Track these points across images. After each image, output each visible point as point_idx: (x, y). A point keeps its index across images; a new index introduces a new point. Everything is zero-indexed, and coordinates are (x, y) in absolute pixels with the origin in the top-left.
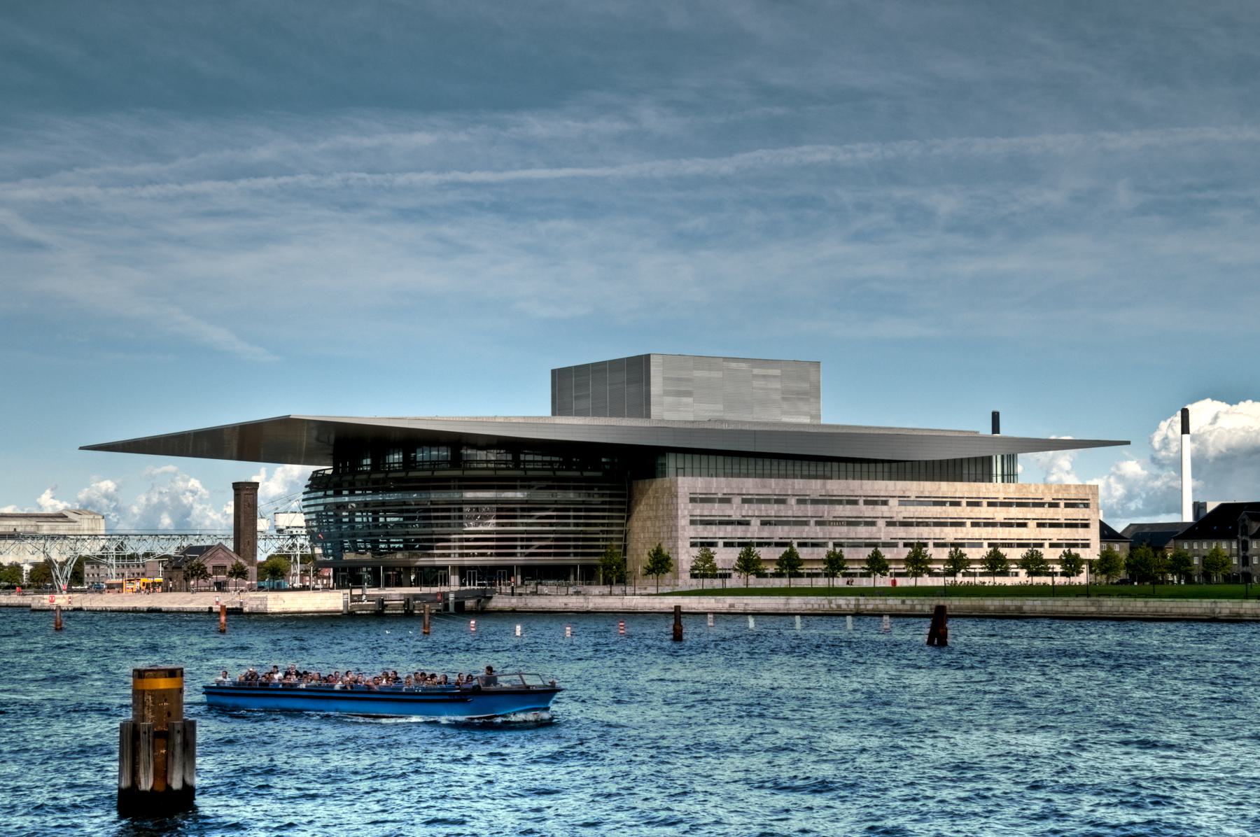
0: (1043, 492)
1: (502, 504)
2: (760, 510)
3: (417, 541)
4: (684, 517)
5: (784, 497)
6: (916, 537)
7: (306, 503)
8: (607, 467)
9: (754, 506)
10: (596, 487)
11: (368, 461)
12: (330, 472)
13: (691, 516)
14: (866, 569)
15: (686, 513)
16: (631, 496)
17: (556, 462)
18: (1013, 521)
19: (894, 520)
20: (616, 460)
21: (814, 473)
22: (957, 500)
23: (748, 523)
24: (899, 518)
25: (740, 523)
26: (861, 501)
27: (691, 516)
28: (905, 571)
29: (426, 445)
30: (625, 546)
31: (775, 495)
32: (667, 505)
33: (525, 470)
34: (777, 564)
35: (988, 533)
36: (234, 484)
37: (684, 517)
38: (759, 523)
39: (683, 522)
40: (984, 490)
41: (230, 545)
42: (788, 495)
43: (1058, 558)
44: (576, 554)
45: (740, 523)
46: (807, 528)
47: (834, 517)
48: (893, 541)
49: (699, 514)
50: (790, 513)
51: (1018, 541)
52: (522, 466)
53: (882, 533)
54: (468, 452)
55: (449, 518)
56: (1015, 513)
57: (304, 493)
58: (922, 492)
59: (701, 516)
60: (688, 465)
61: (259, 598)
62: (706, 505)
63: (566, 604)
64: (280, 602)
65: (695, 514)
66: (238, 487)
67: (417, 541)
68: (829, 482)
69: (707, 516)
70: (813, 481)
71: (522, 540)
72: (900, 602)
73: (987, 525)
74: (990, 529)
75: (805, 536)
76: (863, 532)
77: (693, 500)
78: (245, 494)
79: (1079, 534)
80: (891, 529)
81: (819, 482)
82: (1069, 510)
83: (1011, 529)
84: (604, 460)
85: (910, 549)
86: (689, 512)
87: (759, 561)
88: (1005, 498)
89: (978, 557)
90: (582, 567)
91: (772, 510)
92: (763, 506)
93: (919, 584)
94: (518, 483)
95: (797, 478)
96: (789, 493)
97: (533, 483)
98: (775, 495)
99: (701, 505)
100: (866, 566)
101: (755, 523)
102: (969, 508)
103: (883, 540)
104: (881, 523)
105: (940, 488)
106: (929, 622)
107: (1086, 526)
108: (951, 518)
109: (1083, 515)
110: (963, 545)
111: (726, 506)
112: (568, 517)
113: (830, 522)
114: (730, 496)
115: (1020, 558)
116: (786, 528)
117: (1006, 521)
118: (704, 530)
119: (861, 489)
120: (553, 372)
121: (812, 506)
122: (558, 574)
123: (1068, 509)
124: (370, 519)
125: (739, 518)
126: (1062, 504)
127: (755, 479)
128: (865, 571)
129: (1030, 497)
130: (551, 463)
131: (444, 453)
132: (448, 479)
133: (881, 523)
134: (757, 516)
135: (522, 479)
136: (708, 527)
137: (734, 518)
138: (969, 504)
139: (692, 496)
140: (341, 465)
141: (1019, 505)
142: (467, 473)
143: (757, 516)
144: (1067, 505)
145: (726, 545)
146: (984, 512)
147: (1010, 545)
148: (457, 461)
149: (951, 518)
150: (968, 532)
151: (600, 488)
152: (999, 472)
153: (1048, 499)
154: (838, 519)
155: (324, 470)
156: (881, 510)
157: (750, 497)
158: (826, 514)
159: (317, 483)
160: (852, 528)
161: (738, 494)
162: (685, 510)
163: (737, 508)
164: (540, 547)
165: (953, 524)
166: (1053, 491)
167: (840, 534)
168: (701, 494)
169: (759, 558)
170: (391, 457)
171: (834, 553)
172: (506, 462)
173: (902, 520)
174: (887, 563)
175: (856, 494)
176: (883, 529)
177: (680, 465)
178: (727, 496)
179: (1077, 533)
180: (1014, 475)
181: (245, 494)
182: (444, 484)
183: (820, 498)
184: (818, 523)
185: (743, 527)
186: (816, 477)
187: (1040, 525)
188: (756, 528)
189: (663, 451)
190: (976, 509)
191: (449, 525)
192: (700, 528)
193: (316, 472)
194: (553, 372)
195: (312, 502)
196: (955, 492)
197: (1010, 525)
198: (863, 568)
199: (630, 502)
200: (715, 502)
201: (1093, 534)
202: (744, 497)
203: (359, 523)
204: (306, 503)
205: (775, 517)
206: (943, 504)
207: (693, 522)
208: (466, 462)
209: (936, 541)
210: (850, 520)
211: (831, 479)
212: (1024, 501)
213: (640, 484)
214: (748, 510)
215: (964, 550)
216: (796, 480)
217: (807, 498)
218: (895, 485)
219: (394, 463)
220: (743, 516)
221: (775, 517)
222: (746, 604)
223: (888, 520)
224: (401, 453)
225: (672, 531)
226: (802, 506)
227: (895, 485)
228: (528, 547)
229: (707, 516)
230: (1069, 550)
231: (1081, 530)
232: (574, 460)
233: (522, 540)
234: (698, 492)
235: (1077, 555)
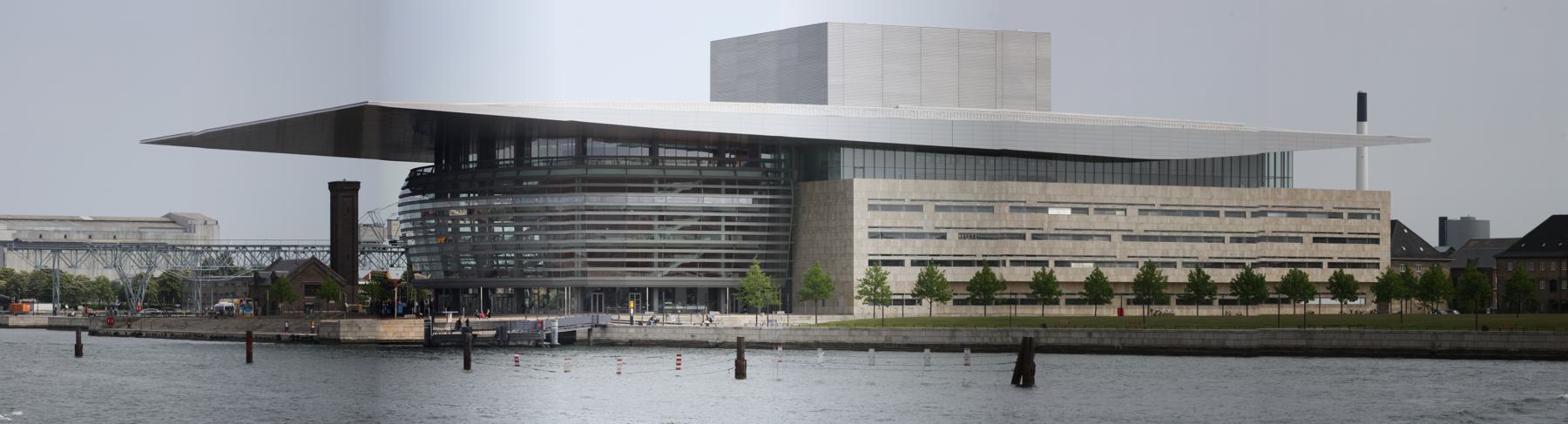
0: (1321, 200)
1: (634, 210)
2: (959, 220)
3: (540, 256)
4: (862, 228)
5: (990, 204)
6: (1161, 255)
7: (402, 209)
8: (768, 165)
9: (951, 215)
10: (756, 190)
11: (473, 157)
12: (429, 170)
14: (1085, 294)
15: (864, 223)
16: (797, 201)
17: (705, 159)
18: (1284, 235)
19: (1134, 234)
20: (783, 157)
21: (1025, 173)
22: (1214, 209)
23: (944, 237)
24: (1139, 231)
25: (932, 235)
26: (1091, 211)
28: (965, 297)
29: (542, 138)
30: (791, 264)
31: (978, 201)
32: (841, 214)
33: (664, 168)
34: (968, 289)
35: (1251, 251)
36: (329, 183)
37: (862, 228)
38: (957, 236)
39: (860, 235)
40: (1248, 198)
41: (326, 259)
42: (995, 202)
43: (1327, 281)
44: (728, 275)
45: (932, 235)
46: (1021, 242)
47: (1056, 229)
48: (1131, 260)
49: (879, 225)
50: (997, 225)
51: (1289, 260)
52: (660, 164)
53: (1121, 249)
54: (594, 147)
55: (572, 227)
56: (1287, 224)
57: (401, 197)
58: (1169, 199)
59: (882, 227)
60: (869, 163)
61: (331, 323)
62: (890, 214)
63: (692, 336)
64: (355, 329)
66: (335, 187)
67: (540, 256)
68: (1050, 185)
69: (891, 227)
70: (1030, 184)
71: (660, 255)
72: (1085, 335)
73: (1251, 240)
74: (1254, 246)
75: (1018, 253)
76: (1093, 247)
77: (872, 207)
78: (344, 196)
79: (1367, 251)
80: (1129, 244)
81: (1038, 185)
82: (1355, 222)
83: (1280, 244)
84: (764, 156)
85: (918, 270)
87: (945, 284)
88: (1274, 207)
89: (1125, 279)
90: (732, 290)
91: (975, 220)
92: (962, 215)
93: (1098, 314)
94: (656, 185)
95: (1013, 180)
96: (996, 199)
97: (674, 185)
98: (978, 201)
99: (883, 213)
100: (1084, 291)
101: (952, 236)
102: (1228, 219)
103: (1118, 259)
104: (1116, 237)
105: (1191, 194)
106: (1014, 358)
107: (1376, 241)
108: (1205, 232)
109: (1372, 228)
110: (995, 264)
111: (916, 214)
112: (718, 228)
113: (1051, 235)
114: (920, 203)
115: (1280, 280)
116: (992, 242)
117: (1274, 234)
119: (1092, 195)
120: (715, 46)
121: (1029, 214)
122: (714, 299)
123: (1353, 220)
124: (477, 229)
125: (932, 230)
126: (1345, 216)
127: (955, 182)
128: (1084, 297)
129: (1306, 204)
130: (699, 160)
131: (566, 147)
132: (571, 180)
133: (1116, 237)
134: (954, 228)
135: (661, 181)
136: (892, 240)
137: (925, 230)
138: (1228, 214)
139: (871, 202)
140: (444, 162)
141: (1291, 214)
142: (593, 172)
143: (954, 228)
144: (1351, 216)
145: (914, 263)
146: (1249, 225)
147: (1219, 265)
148: (581, 156)
149: (1205, 232)
150: (1062, 248)
151: (761, 192)
152: (1272, 174)
153: (1328, 208)
154: (1061, 232)
155: (423, 168)
156: (1118, 220)
157: (945, 204)
158: (1046, 226)
159: (415, 183)
160: (1078, 242)
161: (931, 201)
162: (862, 219)
163: (928, 217)
164: (684, 265)
165: (1209, 240)
166: (1334, 199)
167: (1064, 250)
168: (882, 200)
169: (943, 279)
170: (501, 151)
171: (1043, 274)
172: (642, 158)
173: (1143, 234)
174: (1112, 286)
175: (1084, 201)
176: (1118, 246)
177: (859, 163)
179: (1364, 250)
180: (1288, 178)
181: (344, 196)
182: (565, 186)
183: (1039, 205)
184: (1035, 237)
185: (938, 242)
186: (1037, 179)
187: (1316, 240)
188: (954, 242)
189: (836, 146)
190: (1238, 220)
191: (572, 237)
193: (414, 171)
194: (715, 46)
195: (408, 208)
196: (1211, 199)
197: (1280, 239)
198: (1081, 293)
199: (796, 209)
200: (901, 210)
201: (1383, 252)
202: (938, 204)
203: (466, 233)
204: (402, 209)
205: (978, 228)
206: (1196, 214)
207: (873, 236)
208: (593, 157)
209: (1186, 260)
211: (1056, 181)
212: (1297, 210)
213: (813, 189)
214: (943, 220)
215: (994, 269)
216: (1010, 183)
217: (1022, 205)
218: (1135, 189)
219: (504, 160)
220: (939, 228)
221: (978, 228)
222: (905, 337)
223: (1125, 233)
224: (513, 147)
225: (845, 246)
226: (1016, 215)
227: (1135, 189)
228: (666, 265)
229: (891, 227)
230: (1341, 271)
231: (1368, 247)
232: (727, 156)
233: (660, 255)
234: (879, 198)
235: (1351, 277)
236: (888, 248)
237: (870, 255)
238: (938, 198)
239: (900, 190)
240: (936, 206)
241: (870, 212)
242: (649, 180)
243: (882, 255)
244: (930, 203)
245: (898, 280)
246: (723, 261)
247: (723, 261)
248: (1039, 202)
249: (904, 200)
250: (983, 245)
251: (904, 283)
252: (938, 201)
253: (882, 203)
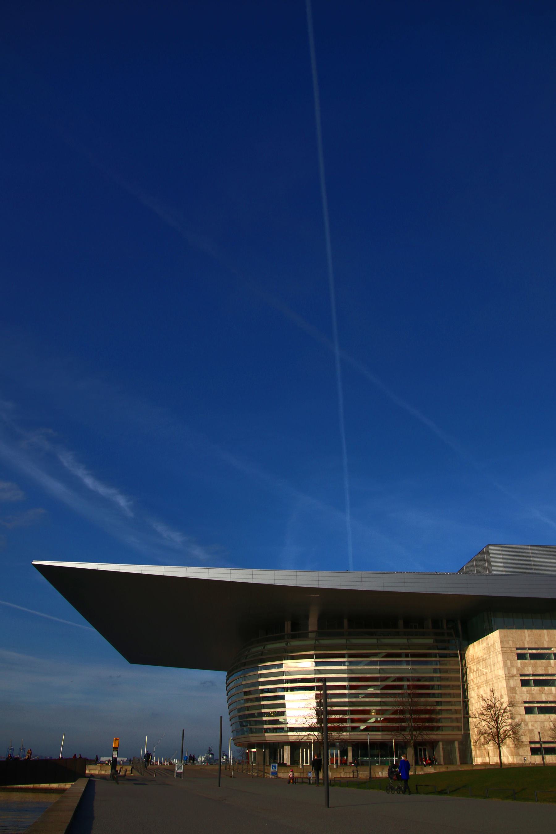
4: (513, 676)
13: (521, 675)
15: (514, 671)
27: (521, 675)
37: (513, 676)
59: (534, 675)
62: (539, 662)
65: (528, 673)
77: (521, 657)
86: (518, 669)
118: (541, 692)
136: (546, 688)
168: (530, 649)
192: (535, 689)
207: (525, 683)
234: (526, 646)
236: (543, 695)
237: (525, 702)
239: (547, 639)
241: (519, 661)
243: (538, 702)
249: (549, 649)
253: (530, 651)
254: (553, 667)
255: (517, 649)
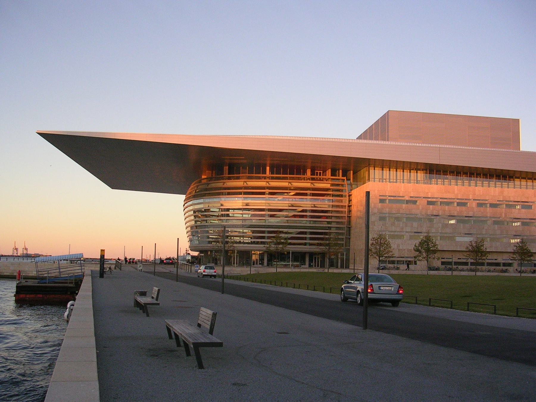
4: (375, 214)
5: (466, 201)
161: (424, 198)
175: (529, 200)
178: (413, 199)
183: (498, 203)
202: (430, 200)
210: (525, 221)
217: (487, 202)
238: (429, 196)
240: (428, 201)
242: (263, 188)
244: (424, 199)
245: (401, 248)
246: (308, 236)
247: (308, 236)
248: (498, 201)
250: (462, 228)
251: (405, 249)
252: (430, 198)
254: (404, 209)
255: (380, 196)
